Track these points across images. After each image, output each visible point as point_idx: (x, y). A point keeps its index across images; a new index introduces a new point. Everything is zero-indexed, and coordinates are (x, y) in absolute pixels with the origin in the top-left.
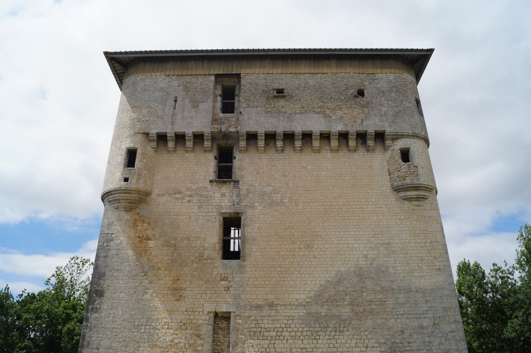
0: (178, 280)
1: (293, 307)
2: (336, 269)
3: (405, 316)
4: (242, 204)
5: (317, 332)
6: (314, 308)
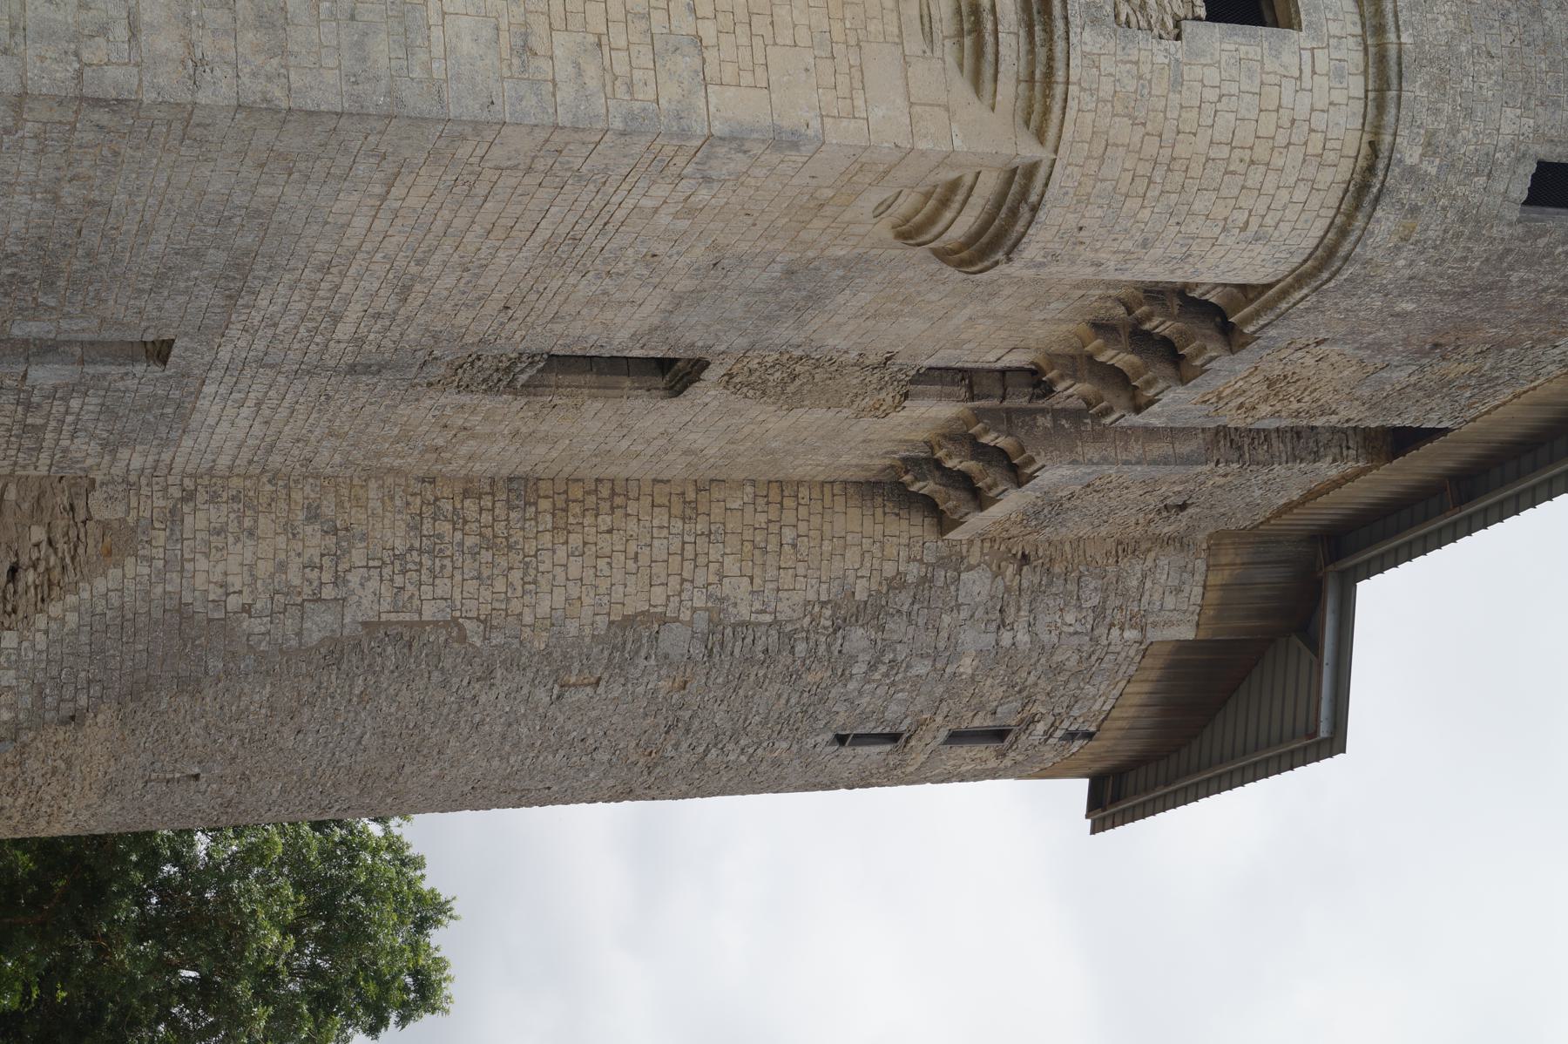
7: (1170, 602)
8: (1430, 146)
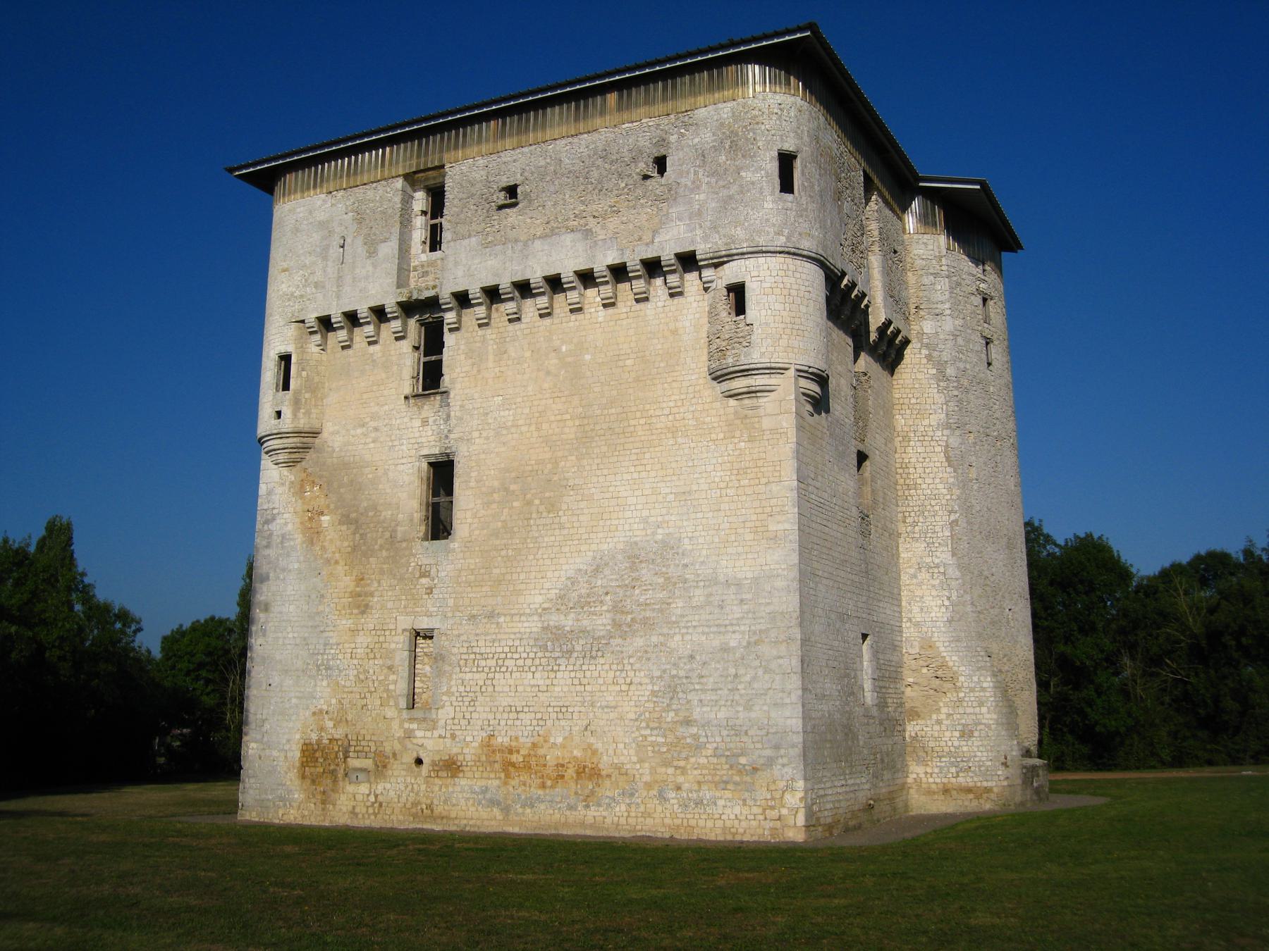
0: (362, 579)
1: (523, 618)
2: (594, 547)
3: (700, 630)
4: (452, 436)
5: (556, 659)
6: (554, 619)
7: (930, 247)
8: (779, 233)
